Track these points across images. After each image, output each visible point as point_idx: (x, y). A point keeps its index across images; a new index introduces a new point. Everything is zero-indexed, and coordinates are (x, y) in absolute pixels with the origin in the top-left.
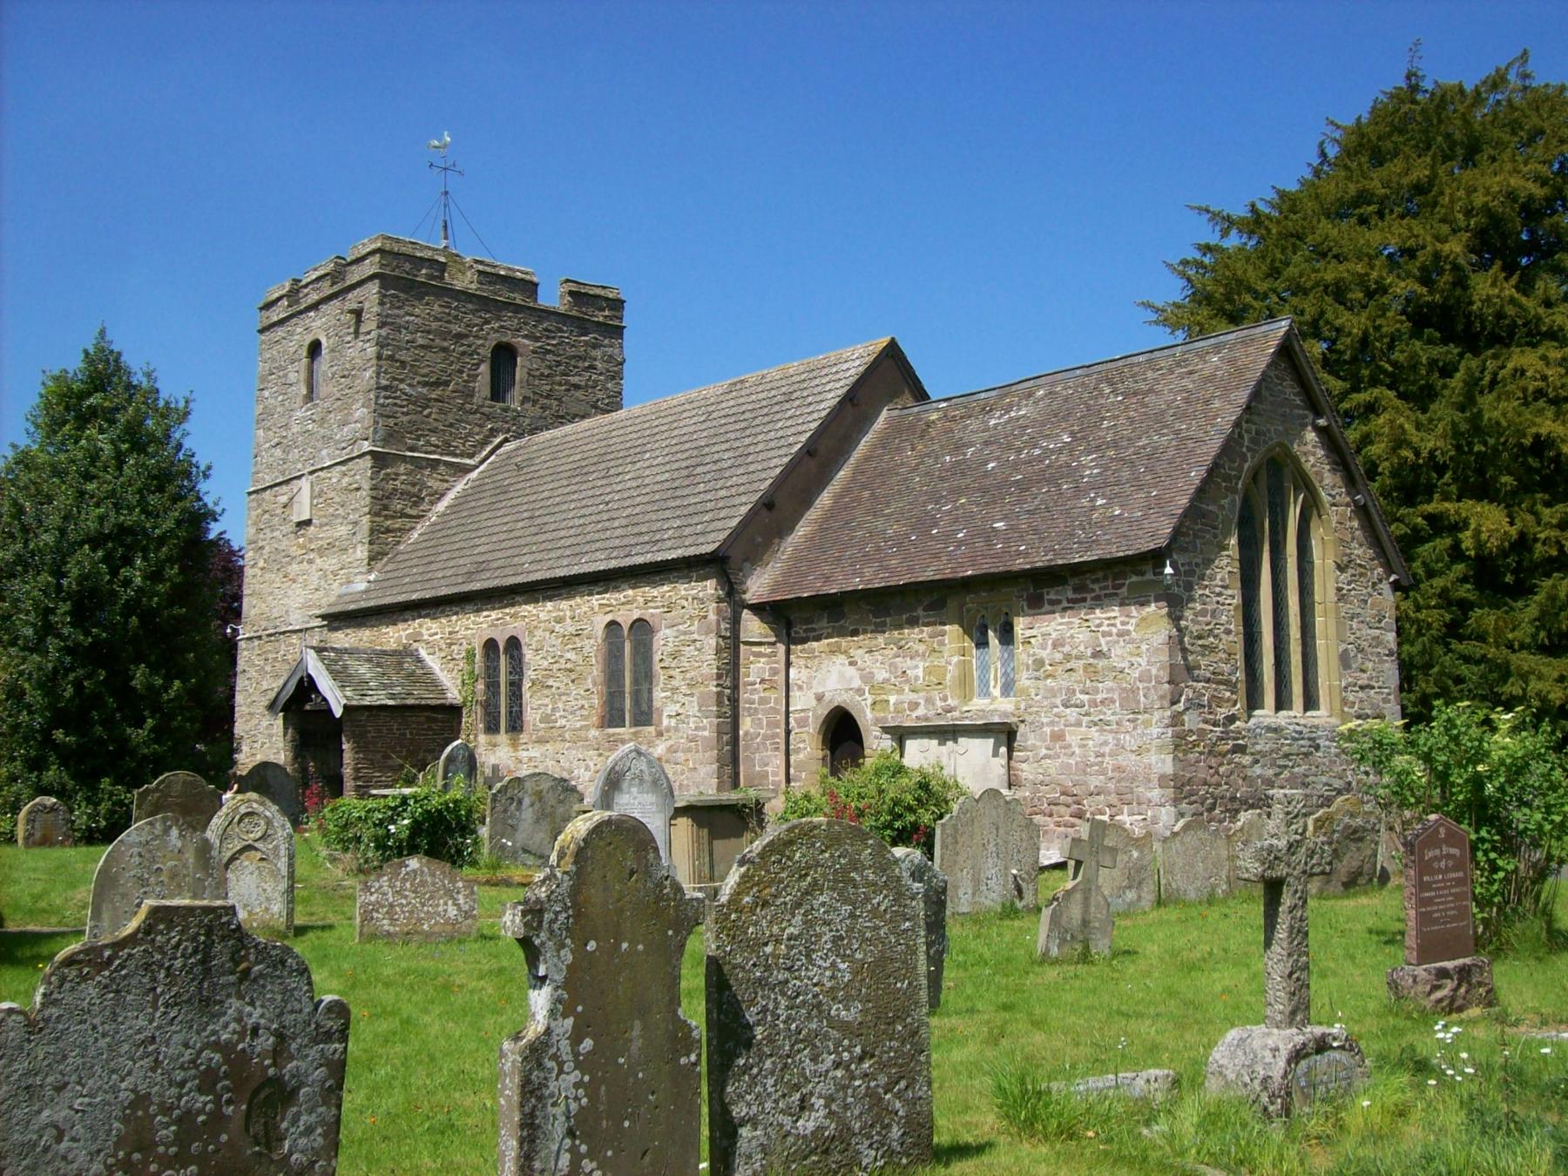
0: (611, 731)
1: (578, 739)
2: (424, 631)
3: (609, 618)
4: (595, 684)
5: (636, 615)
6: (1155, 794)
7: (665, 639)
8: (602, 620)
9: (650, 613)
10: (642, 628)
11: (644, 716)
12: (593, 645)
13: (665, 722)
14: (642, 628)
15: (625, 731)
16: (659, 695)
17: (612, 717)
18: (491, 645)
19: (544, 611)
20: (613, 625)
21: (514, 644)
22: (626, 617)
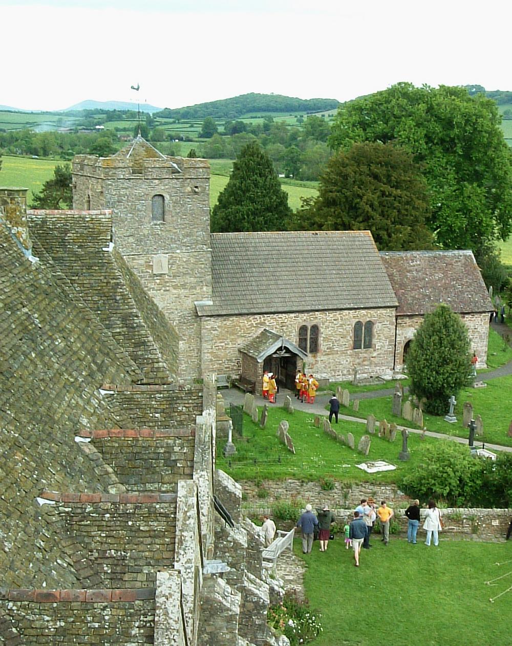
0: (356, 350)
1: (343, 352)
2: (266, 322)
3: (357, 320)
4: (351, 337)
5: (368, 320)
6: (484, 355)
7: (377, 328)
8: (354, 321)
9: (373, 319)
10: (370, 324)
11: (369, 345)
12: (350, 328)
13: (377, 348)
14: (370, 324)
15: (363, 350)
16: (374, 341)
17: (356, 346)
18: (303, 329)
19: (330, 316)
20: (359, 324)
21: (315, 328)
22: (364, 320)
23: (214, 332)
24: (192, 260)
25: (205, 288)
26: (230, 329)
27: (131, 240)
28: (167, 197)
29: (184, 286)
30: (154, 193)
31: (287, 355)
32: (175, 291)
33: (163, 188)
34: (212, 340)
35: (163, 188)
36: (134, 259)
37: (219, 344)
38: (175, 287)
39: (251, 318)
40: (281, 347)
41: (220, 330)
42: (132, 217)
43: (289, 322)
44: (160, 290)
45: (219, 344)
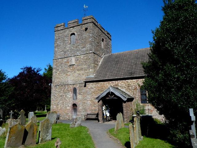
2: (119, 84)
23: (93, 90)
24: (85, 58)
25: (91, 70)
26: (100, 88)
27: (62, 52)
28: (76, 33)
29: (82, 69)
30: (72, 33)
31: (116, 98)
32: (78, 72)
33: (74, 30)
34: (91, 94)
35: (74, 30)
36: (63, 60)
37: (95, 96)
38: (78, 70)
39: (111, 82)
40: (109, 92)
41: (95, 89)
42: (63, 44)
43: (133, 84)
44: (72, 72)
45: (95, 96)
